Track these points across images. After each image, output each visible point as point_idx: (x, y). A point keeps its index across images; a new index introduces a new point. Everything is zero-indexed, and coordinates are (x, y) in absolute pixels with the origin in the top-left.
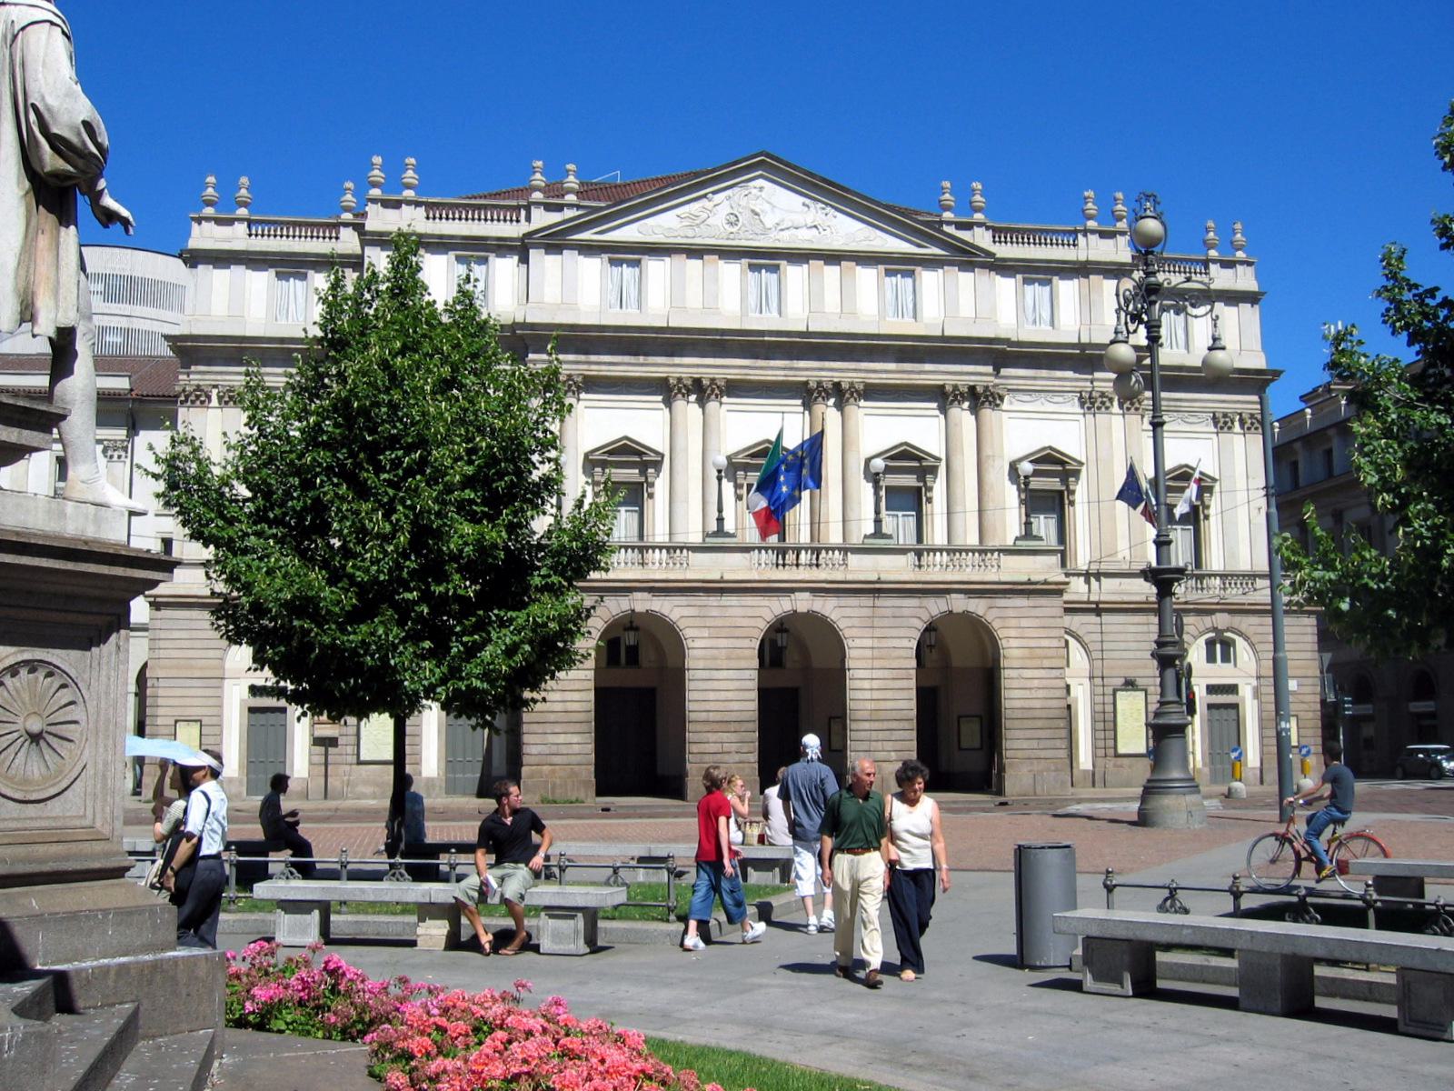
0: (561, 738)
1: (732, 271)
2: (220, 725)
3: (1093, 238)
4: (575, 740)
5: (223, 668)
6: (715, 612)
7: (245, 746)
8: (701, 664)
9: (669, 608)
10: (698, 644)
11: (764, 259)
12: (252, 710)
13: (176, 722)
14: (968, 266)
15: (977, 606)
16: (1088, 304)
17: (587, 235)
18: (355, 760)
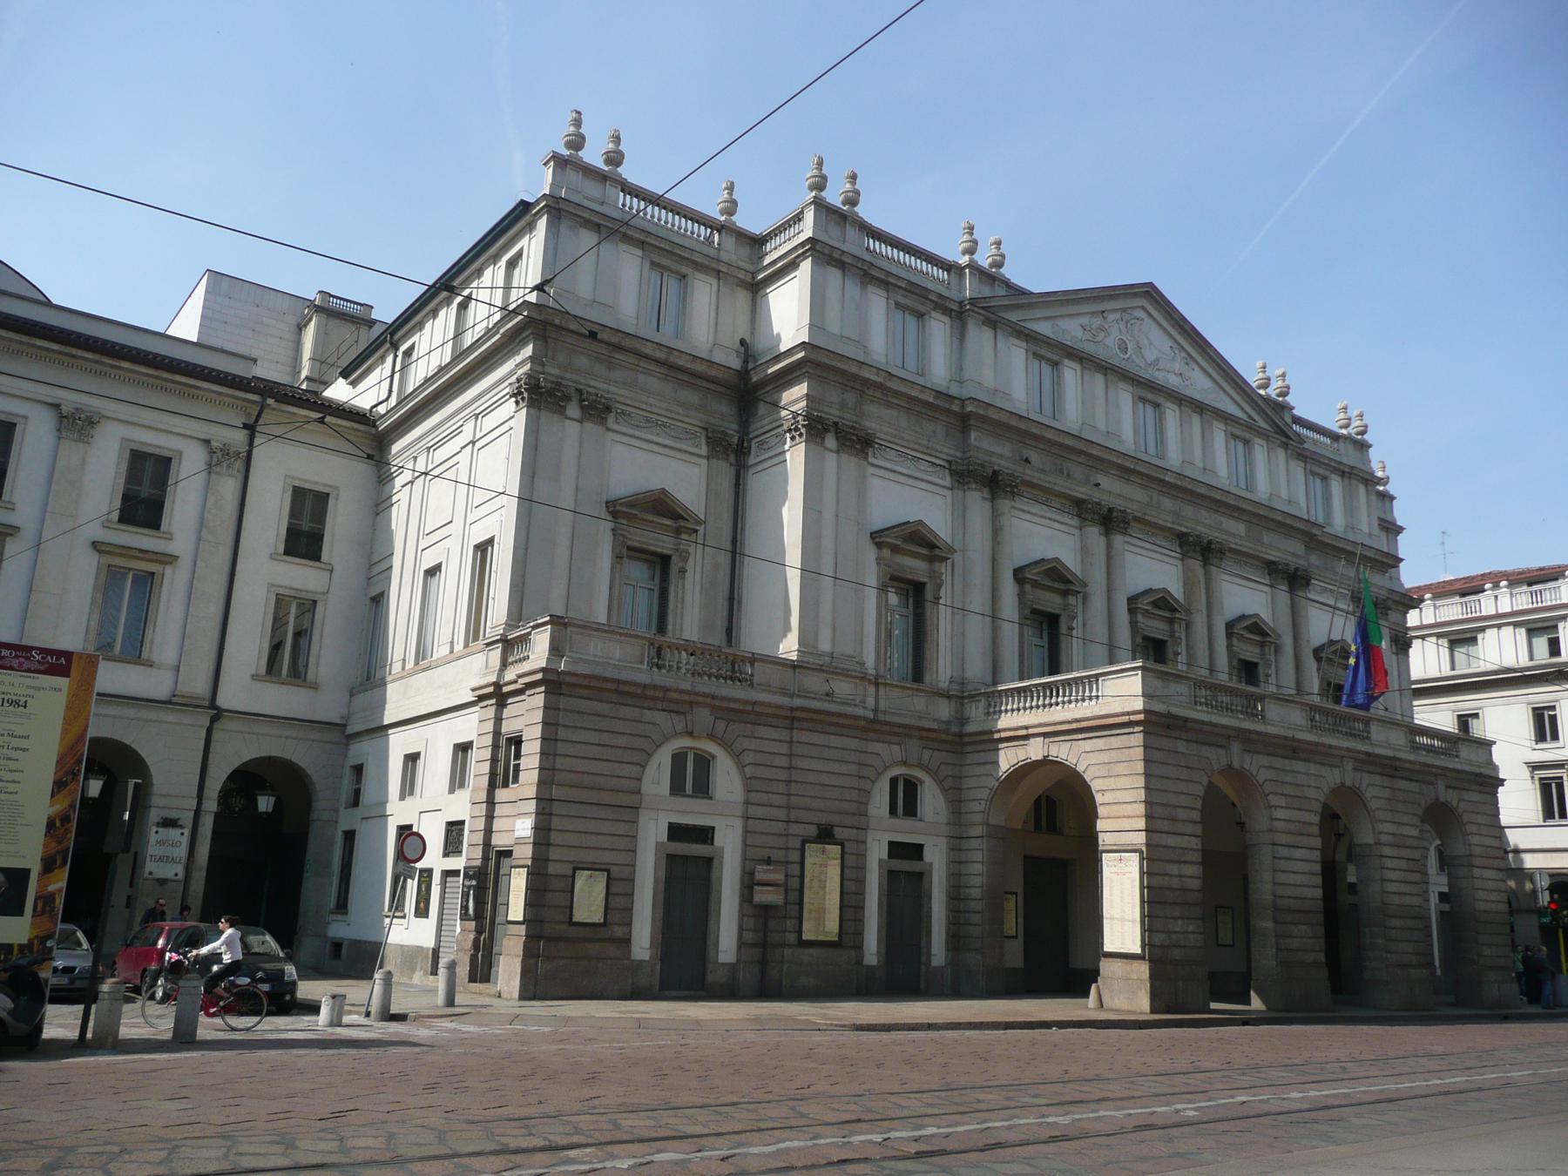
0: (1179, 926)
1: (1125, 396)
2: (631, 881)
3: (1350, 447)
4: (1191, 928)
5: (639, 792)
6: (1288, 779)
7: (660, 912)
8: (1283, 839)
9: (1259, 767)
10: (1280, 814)
11: (1151, 392)
12: (671, 858)
13: (575, 869)
14: (1285, 446)
15: (1451, 797)
16: (1350, 509)
17: (1014, 317)
18: (792, 938)
